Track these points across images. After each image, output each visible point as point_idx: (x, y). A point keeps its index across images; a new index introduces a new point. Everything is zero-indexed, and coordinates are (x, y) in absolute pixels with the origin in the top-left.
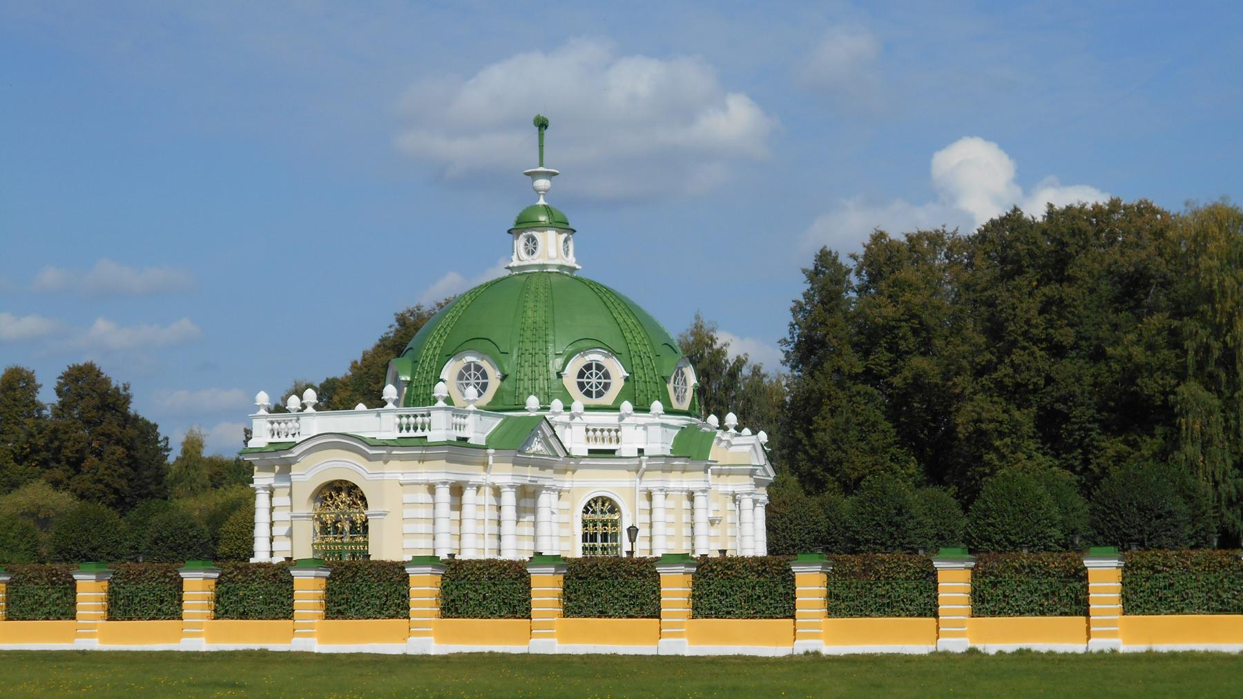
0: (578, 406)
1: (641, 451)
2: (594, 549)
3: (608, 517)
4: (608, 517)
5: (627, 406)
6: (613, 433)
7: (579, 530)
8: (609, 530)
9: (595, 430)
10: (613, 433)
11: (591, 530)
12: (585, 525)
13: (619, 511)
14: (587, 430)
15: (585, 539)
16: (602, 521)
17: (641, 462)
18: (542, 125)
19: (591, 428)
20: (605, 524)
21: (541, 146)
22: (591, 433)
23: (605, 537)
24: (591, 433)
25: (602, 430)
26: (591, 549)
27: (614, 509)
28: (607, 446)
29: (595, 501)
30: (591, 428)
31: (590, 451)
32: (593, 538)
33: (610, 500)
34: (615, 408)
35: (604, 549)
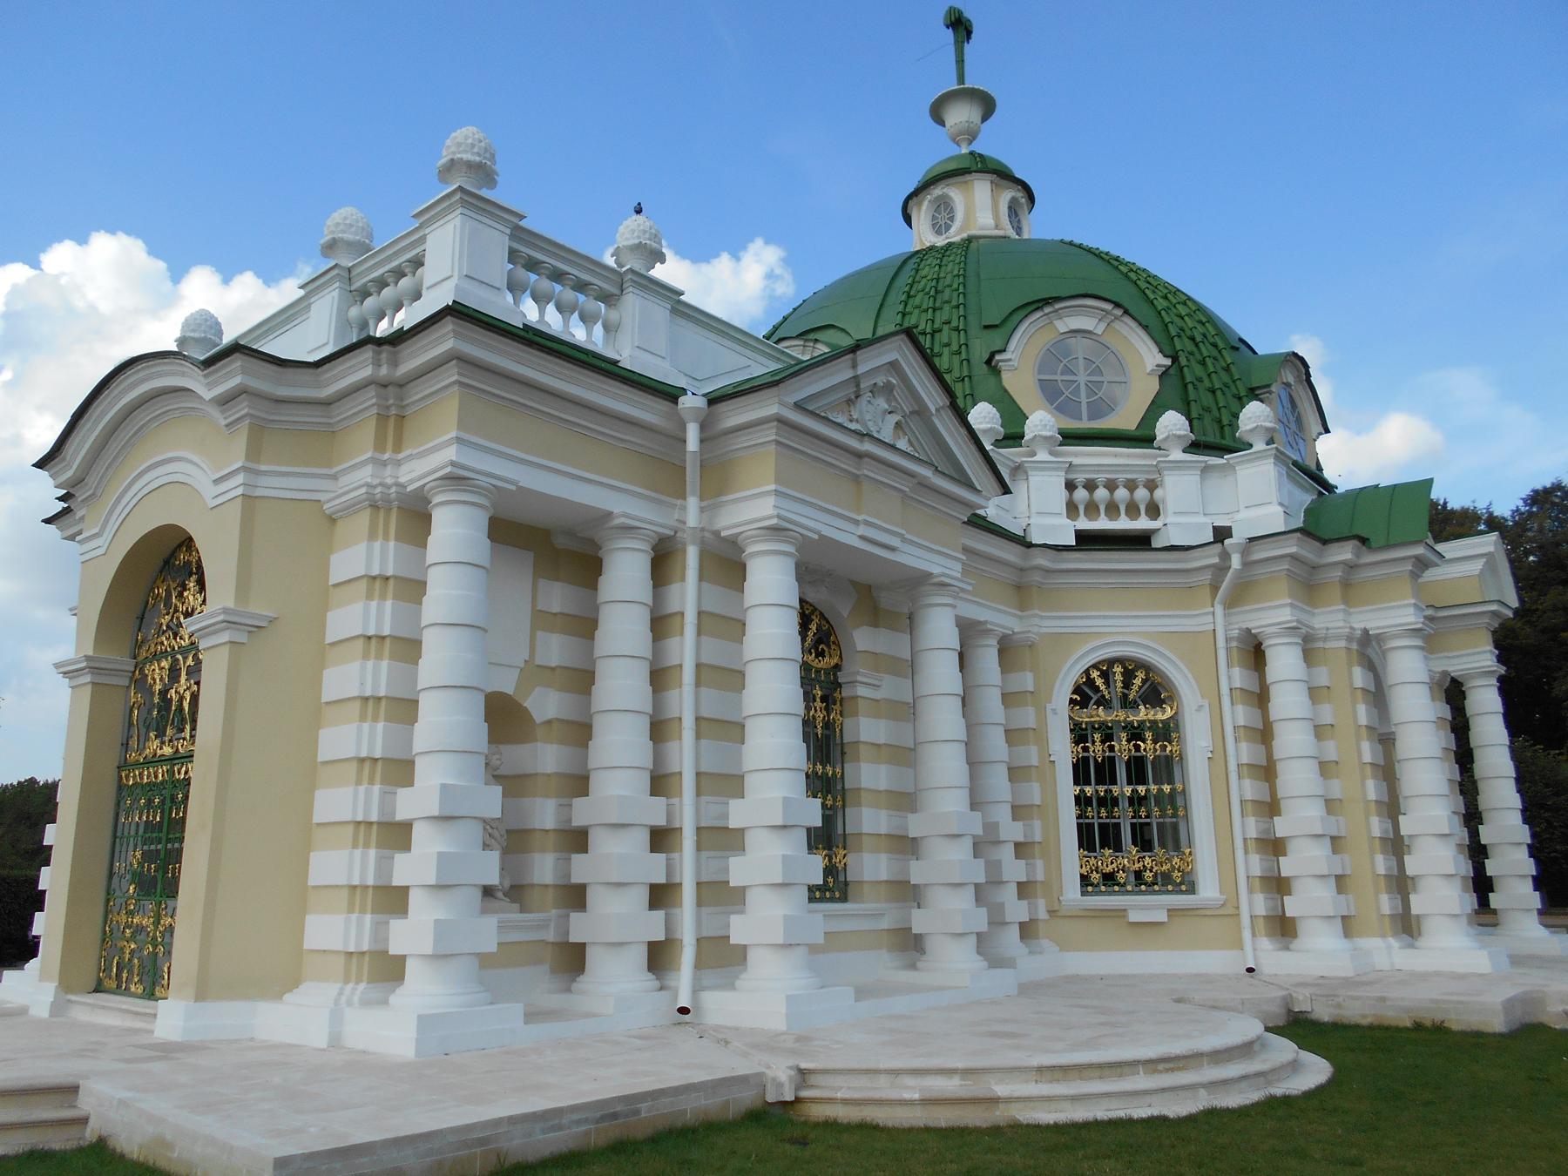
1: (1221, 534)
2: (1109, 802)
3: (1143, 714)
4: (1143, 714)
5: (1172, 423)
6: (1141, 494)
7: (1063, 751)
8: (1148, 748)
9: (1091, 486)
10: (1141, 494)
11: (1097, 750)
12: (1080, 735)
13: (1173, 698)
14: (1070, 486)
15: (1081, 772)
16: (1128, 727)
17: (1225, 556)
18: (959, 25)
19: (1080, 478)
20: (1136, 734)
21: (960, 61)
22: (1081, 494)
23: (1137, 770)
24: (1081, 494)
26: (1102, 802)
27: (1156, 693)
28: (1123, 524)
29: (1105, 668)
30: (1080, 478)
31: (1086, 540)
32: (1106, 772)
33: (1147, 668)
35: (1137, 801)
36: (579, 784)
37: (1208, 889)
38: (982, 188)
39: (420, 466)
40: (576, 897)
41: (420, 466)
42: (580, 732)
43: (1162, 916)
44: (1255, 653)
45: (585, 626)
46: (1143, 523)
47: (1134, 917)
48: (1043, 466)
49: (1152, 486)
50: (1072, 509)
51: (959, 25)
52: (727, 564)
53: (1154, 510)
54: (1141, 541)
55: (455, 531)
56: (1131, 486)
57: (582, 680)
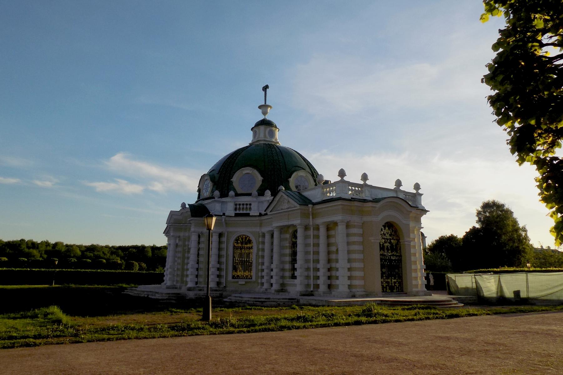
0: (232, 193)
5: (255, 193)
9: (240, 205)
10: (248, 206)
14: (236, 205)
22: (238, 206)
25: (243, 204)
28: (245, 212)
34: (250, 195)
37: (254, 278)
38: (262, 128)
43: (244, 283)
46: (248, 212)
47: (240, 283)
48: (230, 202)
49: (250, 204)
50: (236, 209)
53: (250, 208)
54: (248, 215)
56: (247, 204)
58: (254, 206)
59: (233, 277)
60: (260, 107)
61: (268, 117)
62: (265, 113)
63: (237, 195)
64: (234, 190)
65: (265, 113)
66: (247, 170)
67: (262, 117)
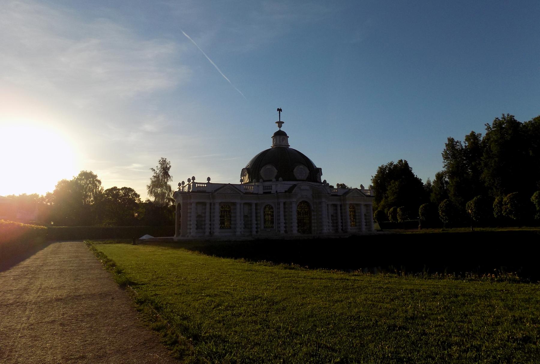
0: (261, 180)
5: (274, 180)
18: (280, 110)
28: (269, 191)
31: (265, 193)
34: (271, 181)
36: (205, 221)
39: (192, 201)
40: (205, 228)
41: (192, 201)
42: (205, 217)
44: (279, 204)
45: (205, 209)
50: (264, 189)
51: (280, 110)
52: (214, 204)
54: (270, 193)
55: (194, 205)
57: (205, 213)
58: (274, 187)
59: (264, 228)
60: (277, 122)
61: (282, 129)
62: (280, 126)
63: (264, 181)
64: (262, 178)
65: (280, 126)
66: (269, 167)
67: (278, 129)
